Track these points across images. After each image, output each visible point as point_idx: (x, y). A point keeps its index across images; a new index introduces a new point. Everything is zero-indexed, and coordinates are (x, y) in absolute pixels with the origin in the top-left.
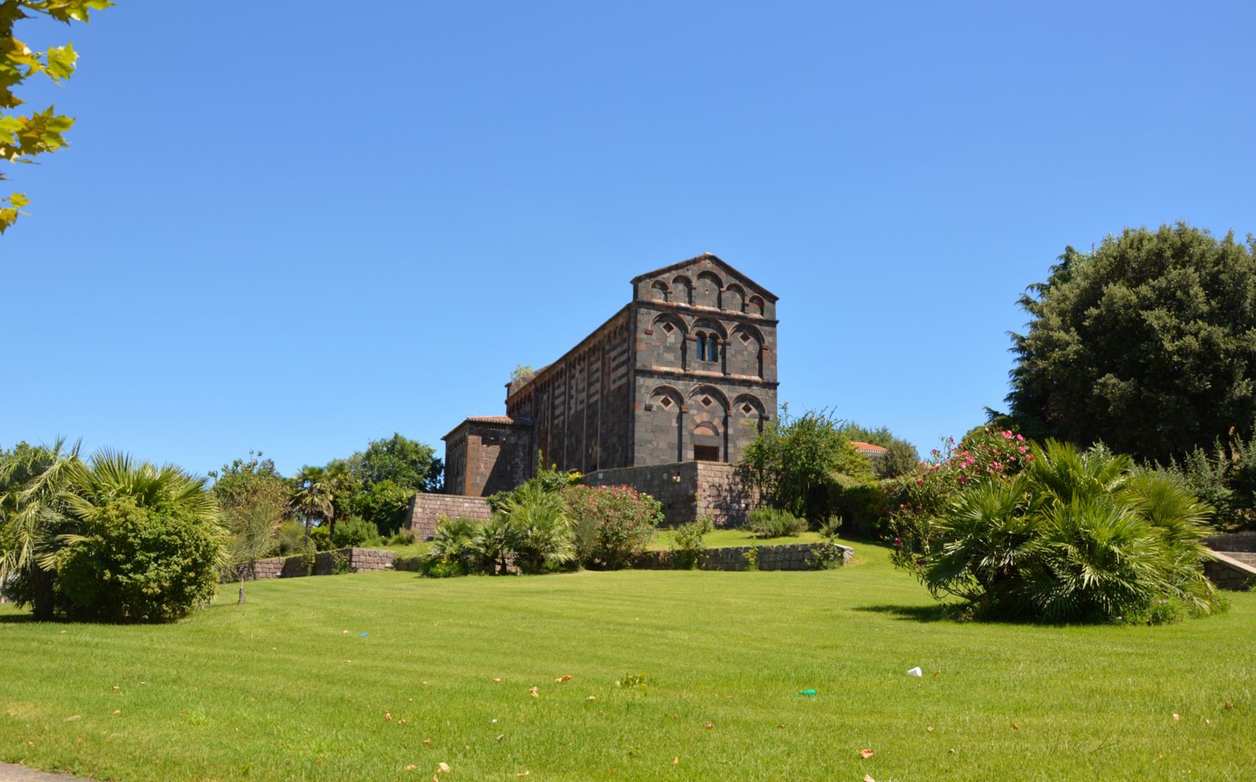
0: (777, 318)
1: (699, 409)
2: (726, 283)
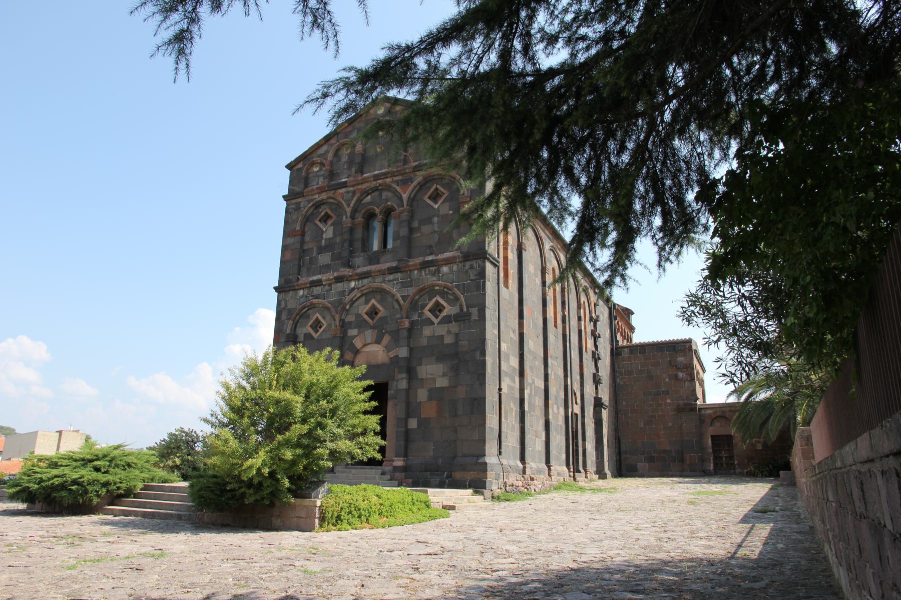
1: (361, 325)
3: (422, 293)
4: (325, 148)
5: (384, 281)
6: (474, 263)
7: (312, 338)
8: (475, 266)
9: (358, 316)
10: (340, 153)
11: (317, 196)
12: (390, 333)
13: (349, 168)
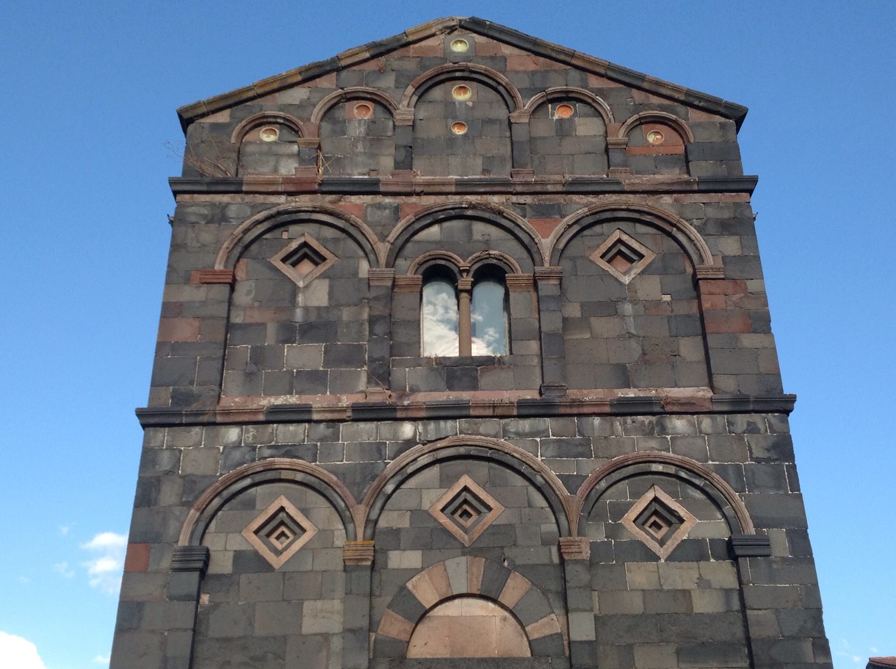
0: (747, 172)
2: (528, 92)
3: (616, 476)
4: (298, 95)
5: (505, 433)
6: (757, 418)
7: (265, 566)
8: (761, 426)
9: (418, 514)
10: (339, 113)
11: (283, 199)
12: (527, 570)
13: (373, 156)
